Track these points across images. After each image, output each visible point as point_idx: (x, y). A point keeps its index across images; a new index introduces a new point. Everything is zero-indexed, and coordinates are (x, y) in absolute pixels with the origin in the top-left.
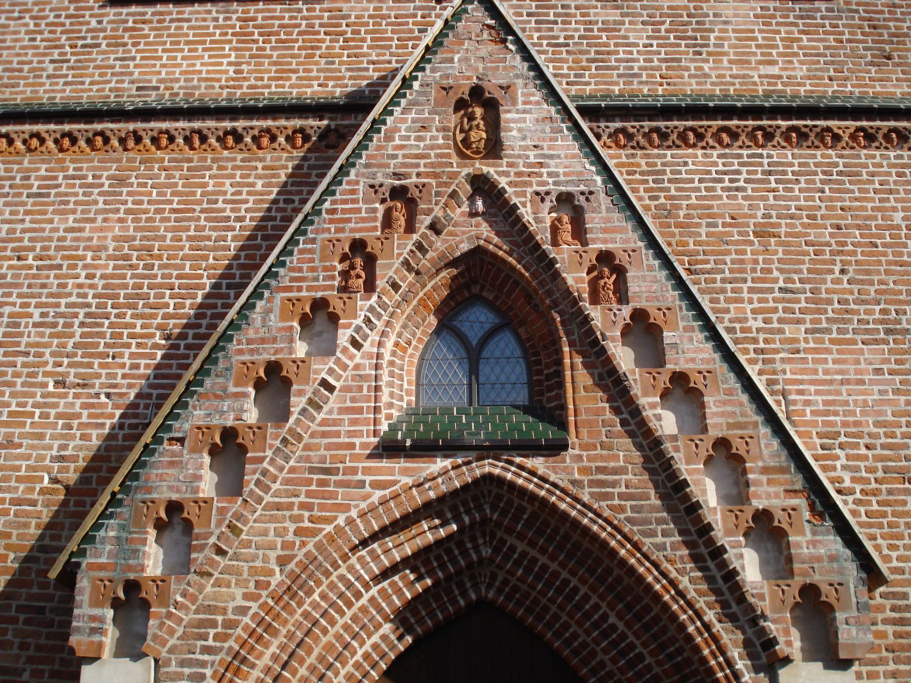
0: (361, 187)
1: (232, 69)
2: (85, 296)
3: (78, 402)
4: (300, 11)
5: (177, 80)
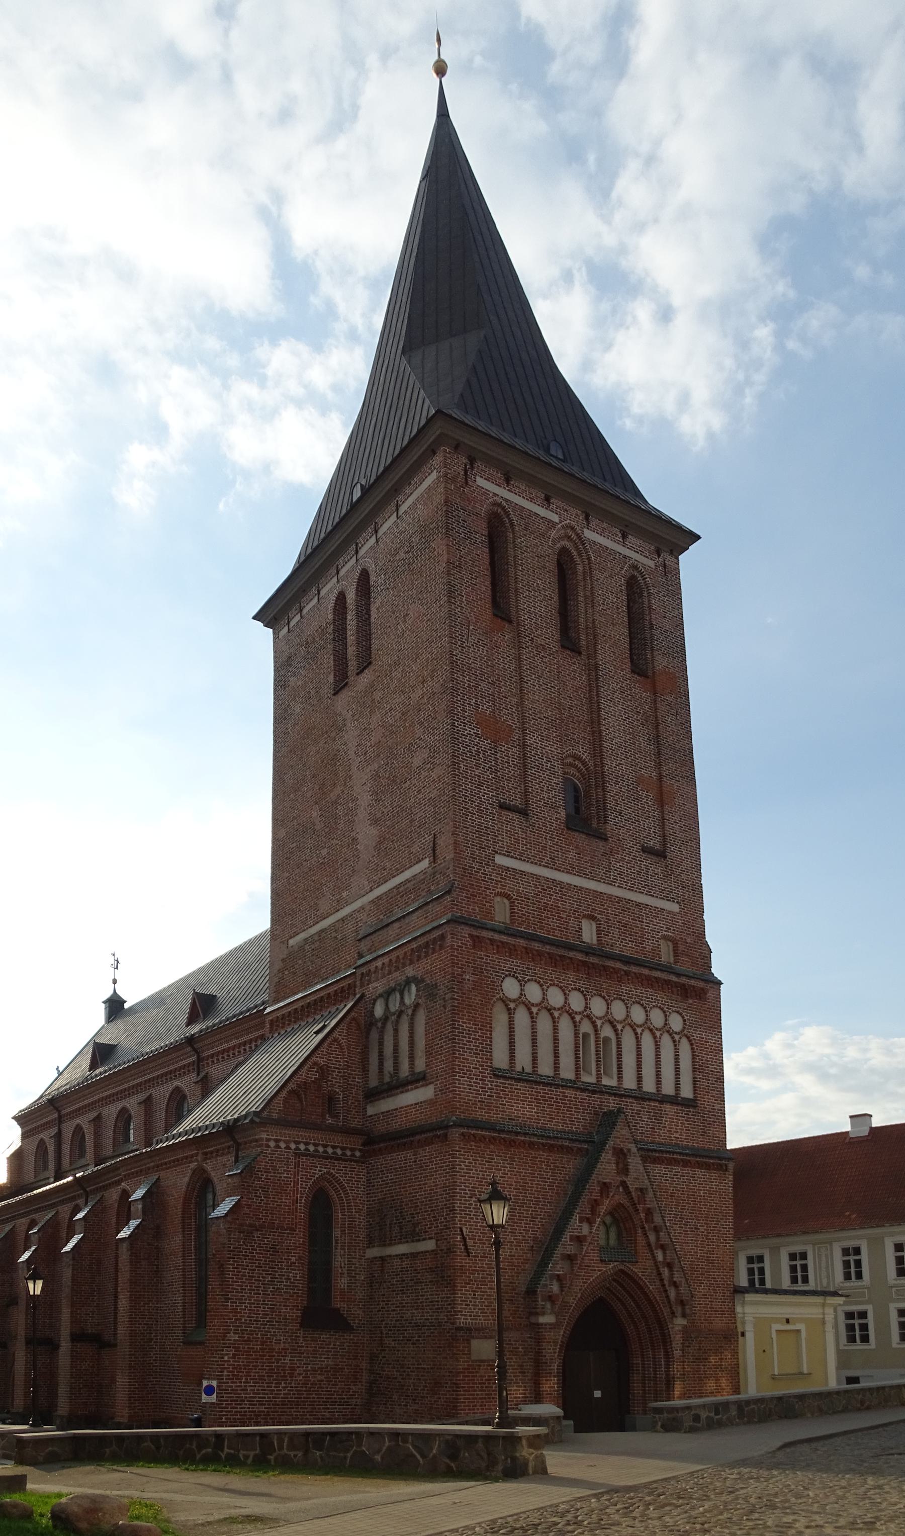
1: (536, 1115)
5: (520, 1117)
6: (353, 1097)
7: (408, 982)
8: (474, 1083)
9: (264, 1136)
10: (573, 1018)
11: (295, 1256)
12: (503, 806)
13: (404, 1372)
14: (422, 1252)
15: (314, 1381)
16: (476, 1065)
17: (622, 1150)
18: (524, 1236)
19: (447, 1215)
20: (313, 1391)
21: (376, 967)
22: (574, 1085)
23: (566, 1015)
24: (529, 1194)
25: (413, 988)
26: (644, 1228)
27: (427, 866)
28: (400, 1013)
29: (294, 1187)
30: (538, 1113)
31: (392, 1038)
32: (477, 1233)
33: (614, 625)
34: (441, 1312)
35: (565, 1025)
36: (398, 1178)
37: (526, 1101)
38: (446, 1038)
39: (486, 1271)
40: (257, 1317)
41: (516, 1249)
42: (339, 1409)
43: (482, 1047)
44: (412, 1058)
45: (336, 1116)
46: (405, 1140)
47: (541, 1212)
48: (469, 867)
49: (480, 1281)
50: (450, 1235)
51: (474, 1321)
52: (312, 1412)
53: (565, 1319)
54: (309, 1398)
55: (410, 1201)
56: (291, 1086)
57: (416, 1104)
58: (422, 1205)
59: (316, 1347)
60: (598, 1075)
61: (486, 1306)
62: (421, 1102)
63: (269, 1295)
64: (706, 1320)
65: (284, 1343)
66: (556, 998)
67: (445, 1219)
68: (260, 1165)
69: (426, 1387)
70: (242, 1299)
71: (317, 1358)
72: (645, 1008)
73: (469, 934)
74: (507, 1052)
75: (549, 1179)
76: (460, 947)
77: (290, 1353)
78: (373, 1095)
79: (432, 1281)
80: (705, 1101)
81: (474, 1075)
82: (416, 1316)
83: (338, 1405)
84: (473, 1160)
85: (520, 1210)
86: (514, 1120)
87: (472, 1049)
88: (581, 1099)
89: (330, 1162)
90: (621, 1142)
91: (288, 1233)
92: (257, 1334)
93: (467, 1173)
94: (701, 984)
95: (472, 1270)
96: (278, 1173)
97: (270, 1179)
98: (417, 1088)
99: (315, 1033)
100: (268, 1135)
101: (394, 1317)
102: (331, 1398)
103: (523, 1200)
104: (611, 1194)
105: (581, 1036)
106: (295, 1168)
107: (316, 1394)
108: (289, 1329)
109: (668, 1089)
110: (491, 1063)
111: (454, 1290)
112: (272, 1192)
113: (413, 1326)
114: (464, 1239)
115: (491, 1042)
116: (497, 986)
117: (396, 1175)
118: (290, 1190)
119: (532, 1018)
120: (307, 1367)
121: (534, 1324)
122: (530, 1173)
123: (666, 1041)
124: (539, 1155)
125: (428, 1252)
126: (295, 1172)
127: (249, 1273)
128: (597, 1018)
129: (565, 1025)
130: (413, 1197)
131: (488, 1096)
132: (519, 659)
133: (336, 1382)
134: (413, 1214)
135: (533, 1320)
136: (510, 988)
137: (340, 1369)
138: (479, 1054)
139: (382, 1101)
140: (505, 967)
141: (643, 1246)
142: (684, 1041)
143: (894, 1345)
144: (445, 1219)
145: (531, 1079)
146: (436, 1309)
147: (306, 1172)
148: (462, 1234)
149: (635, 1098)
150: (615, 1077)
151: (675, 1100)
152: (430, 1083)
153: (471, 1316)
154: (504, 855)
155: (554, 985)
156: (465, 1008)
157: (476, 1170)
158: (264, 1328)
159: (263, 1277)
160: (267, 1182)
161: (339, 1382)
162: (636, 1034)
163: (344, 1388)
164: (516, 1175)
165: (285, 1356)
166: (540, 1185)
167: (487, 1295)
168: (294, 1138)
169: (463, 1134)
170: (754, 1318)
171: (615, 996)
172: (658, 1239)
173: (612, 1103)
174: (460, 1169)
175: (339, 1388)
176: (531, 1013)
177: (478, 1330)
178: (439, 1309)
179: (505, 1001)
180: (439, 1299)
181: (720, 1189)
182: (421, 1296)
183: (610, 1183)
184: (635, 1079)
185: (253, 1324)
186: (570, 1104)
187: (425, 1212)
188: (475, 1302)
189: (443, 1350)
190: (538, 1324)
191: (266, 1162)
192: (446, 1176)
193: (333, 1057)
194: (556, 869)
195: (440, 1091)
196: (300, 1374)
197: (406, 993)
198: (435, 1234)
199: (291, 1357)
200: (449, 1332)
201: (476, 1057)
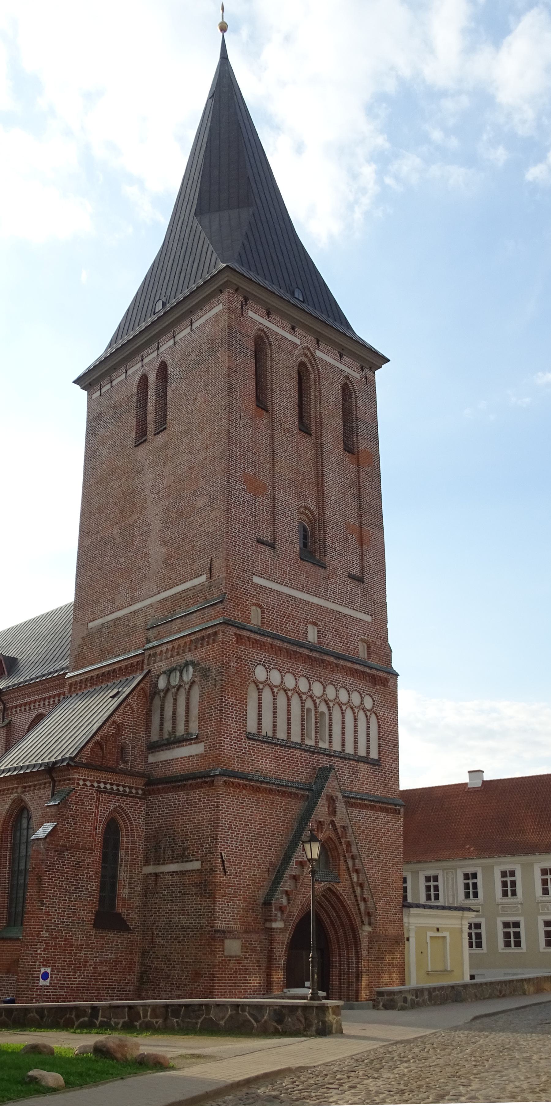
0: (314, 820)
1: (274, 768)
2: (254, 834)
3: (256, 861)
4: (286, 751)
5: (263, 770)
6: (138, 748)
7: (187, 664)
8: (234, 743)
9: (76, 776)
10: (301, 697)
11: (93, 871)
12: (259, 541)
13: (171, 964)
14: (189, 871)
15: (100, 971)
16: (236, 729)
17: (332, 797)
18: (263, 861)
19: (210, 842)
20: (100, 979)
21: (161, 651)
22: (300, 747)
23: (296, 694)
24: (268, 828)
25: (191, 669)
26: (345, 856)
27: (205, 580)
28: (180, 687)
29: (95, 816)
30: (275, 767)
31: (172, 705)
32: (232, 857)
33: (334, 417)
34: (203, 918)
35: (295, 702)
36: (172, 812)
37: (268, 758)
38: (215, 708)
39: (237, 886)
40: (63, 919)
41: (258, 870)
42: (117, 994)
43: (240, 717)
44: (187, 721)
45: (126, 762)
46: (179, 784)
47: (276, 842)
48: (236, 584)
49: (232, 894)
50: (213, 858)
51: (227, 926)
52: (97, 996)
53: (290, 925)
54: (97, 985)
55: (181, 830)
56: (97, 738)
57: (189, 757)
58: (191, 834)
59: (103, 944)
60: (316, 739)
61: (235, 914)
62: (193, 756)
63: (73, 901)
64: (384, 928)
65: (81, 940)
66: (290, 682)
67: (210, 845)
68: (72, 799)
69: (188, 976)
70: (53, 904)
71: (104, 952)
72: (348, 691)
73: (234, 633)
74: (256, 721)
75: (281, 817)
76: (228, 642)
77: (85, 948)
78: (154, 747)
79: (197, 894)
80: (386, 762)
81: (234, 737)
82: (182, 921)
83: (117, 991)
84: (231, 801)
85: (261, 840)
86: (260, 772)
87: (233, 718)
88: (305, 757)
89: (121, 798)
90: (332, 791)
91: (89, 853)
92: (62, 933)
93: (226, 811)
94: (385, 675)
95: (228, 886)
96: (84, 806)
97: (78, 810)
98: (191, 744)
99: (111, 697)
100: (79, 776)
101: (164, 921)
102: (112, 985)
103: (264, 833)
104: (324, 830)
105: (305, 710)
106: (96, 802)
107: (101, 982)
108: (85, 929)
109: (362, 752)
110: (246, 729)
111: (215, 901)
112: (79, 820)
113: (179, 929)
114: (223, 861)
115: (246, 713)
116: (252, 672)
117: (171, 810)
118: (92, 819)
119: (274, 696)
120: (96, 960)
121: (269, 928)
122: (269, 812)
123: (361, 716)
124: (275, 799)
125: (194, 870)
126: (96, 805)
127: (59, 883)
128: (317, 697)
129: (295, 702)
130: (184, 827)
131: (243, 753)
132: (272, 437)
133: (116, 972)
134: (183, 840)
135: (268, 925)
136: (260, 673)
137: (119, 961)
138: (238, 722)
139: (162, 752)
140: (257, 658)
141: (344, 870)
142: (373, 716)
143: (500, 951)
144: (210, 845)
145: (271, 741)
146: (199, 915)
147: (104, 805)
148: (222, 858)
149: (341, 757)
150: (327, 741)
151: (366, 760)
152: (201, 742)
153: (225, 921)
154: (259, 576)
155: (289, 672)
156: (229, 687)
157: (233, 809)
158: (68, 928)
159: (69, 887)
160: (76, 812)
161: (118, 972)
162: (342, 710)
163: (121, 977)
164: (260, 814)
165: (81, 951)
166: (276, 821)
167: (237, 905)
168: (97, 778)
169: (225, 782)
170: (416, 927)
171: (329, 682)
172: (354, 865)
173: (324, 762)
174: (222, 808)
175: (118, 977)
176: (273, 692)
177: (229, 932)
178: (201, 915)
179: (256, 683)
180: (202, 908)
181: (394, 828)
182: (187, 905)
183: (324, 822)
184: (340, 744)
185: (60, 924)
186: (297, 761)
187: (193, 839)
188: (228, 910)
189: (203, 948)
190: (271, 929)
191: (76, 797)
192: (211, 813)
193: (127, 717)
194: (292, 588)
195: (209, 748)
196: (91, 965)
197: (184, 672)
198: (201, 857)
199: (85, 951)
200: (209, 934)
201: (236, 724)
